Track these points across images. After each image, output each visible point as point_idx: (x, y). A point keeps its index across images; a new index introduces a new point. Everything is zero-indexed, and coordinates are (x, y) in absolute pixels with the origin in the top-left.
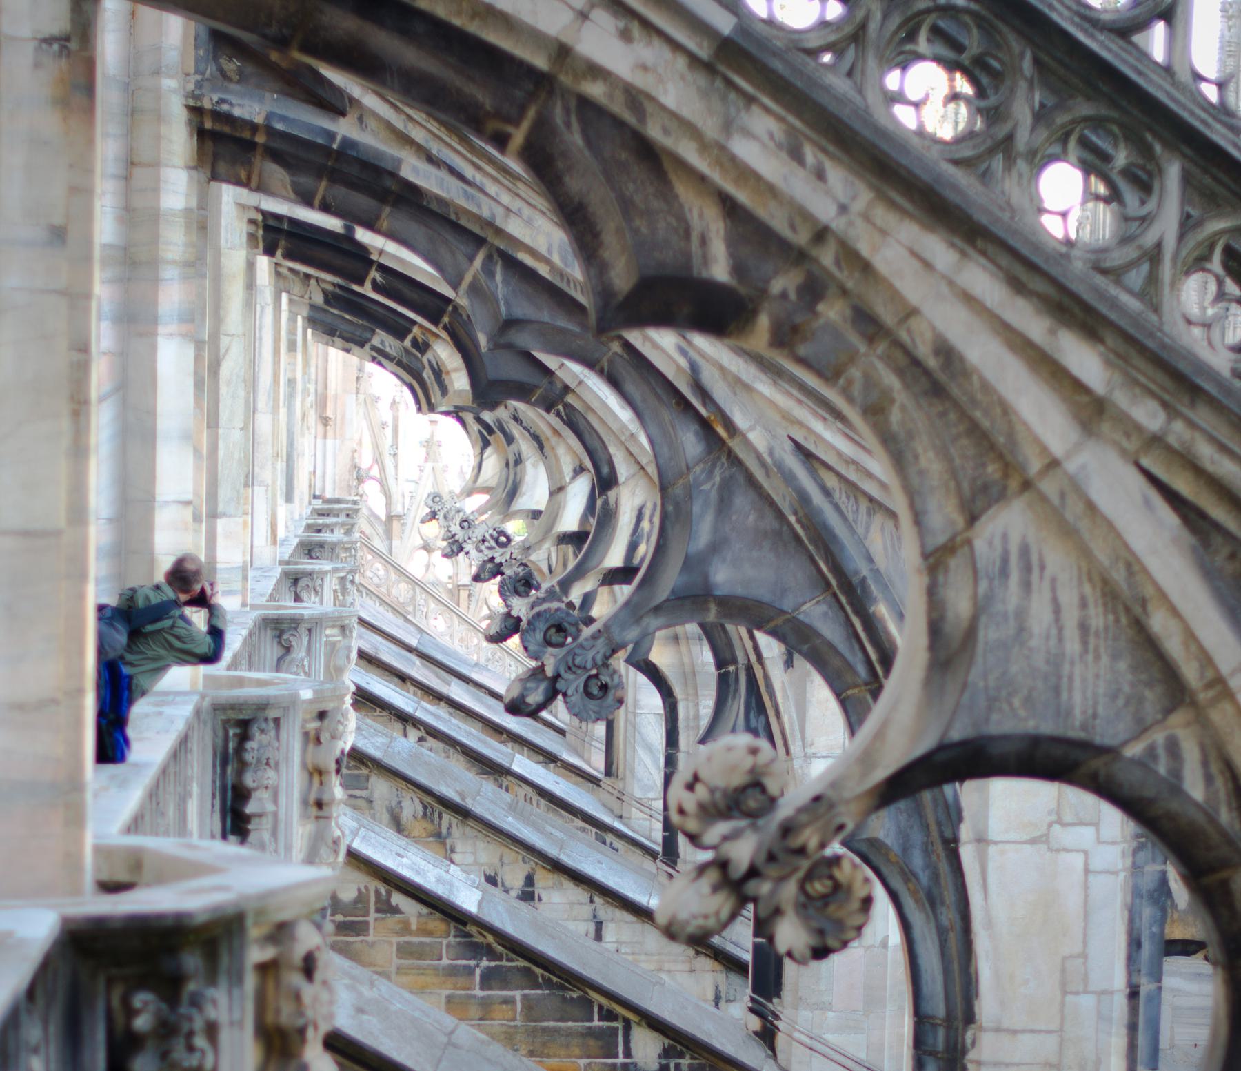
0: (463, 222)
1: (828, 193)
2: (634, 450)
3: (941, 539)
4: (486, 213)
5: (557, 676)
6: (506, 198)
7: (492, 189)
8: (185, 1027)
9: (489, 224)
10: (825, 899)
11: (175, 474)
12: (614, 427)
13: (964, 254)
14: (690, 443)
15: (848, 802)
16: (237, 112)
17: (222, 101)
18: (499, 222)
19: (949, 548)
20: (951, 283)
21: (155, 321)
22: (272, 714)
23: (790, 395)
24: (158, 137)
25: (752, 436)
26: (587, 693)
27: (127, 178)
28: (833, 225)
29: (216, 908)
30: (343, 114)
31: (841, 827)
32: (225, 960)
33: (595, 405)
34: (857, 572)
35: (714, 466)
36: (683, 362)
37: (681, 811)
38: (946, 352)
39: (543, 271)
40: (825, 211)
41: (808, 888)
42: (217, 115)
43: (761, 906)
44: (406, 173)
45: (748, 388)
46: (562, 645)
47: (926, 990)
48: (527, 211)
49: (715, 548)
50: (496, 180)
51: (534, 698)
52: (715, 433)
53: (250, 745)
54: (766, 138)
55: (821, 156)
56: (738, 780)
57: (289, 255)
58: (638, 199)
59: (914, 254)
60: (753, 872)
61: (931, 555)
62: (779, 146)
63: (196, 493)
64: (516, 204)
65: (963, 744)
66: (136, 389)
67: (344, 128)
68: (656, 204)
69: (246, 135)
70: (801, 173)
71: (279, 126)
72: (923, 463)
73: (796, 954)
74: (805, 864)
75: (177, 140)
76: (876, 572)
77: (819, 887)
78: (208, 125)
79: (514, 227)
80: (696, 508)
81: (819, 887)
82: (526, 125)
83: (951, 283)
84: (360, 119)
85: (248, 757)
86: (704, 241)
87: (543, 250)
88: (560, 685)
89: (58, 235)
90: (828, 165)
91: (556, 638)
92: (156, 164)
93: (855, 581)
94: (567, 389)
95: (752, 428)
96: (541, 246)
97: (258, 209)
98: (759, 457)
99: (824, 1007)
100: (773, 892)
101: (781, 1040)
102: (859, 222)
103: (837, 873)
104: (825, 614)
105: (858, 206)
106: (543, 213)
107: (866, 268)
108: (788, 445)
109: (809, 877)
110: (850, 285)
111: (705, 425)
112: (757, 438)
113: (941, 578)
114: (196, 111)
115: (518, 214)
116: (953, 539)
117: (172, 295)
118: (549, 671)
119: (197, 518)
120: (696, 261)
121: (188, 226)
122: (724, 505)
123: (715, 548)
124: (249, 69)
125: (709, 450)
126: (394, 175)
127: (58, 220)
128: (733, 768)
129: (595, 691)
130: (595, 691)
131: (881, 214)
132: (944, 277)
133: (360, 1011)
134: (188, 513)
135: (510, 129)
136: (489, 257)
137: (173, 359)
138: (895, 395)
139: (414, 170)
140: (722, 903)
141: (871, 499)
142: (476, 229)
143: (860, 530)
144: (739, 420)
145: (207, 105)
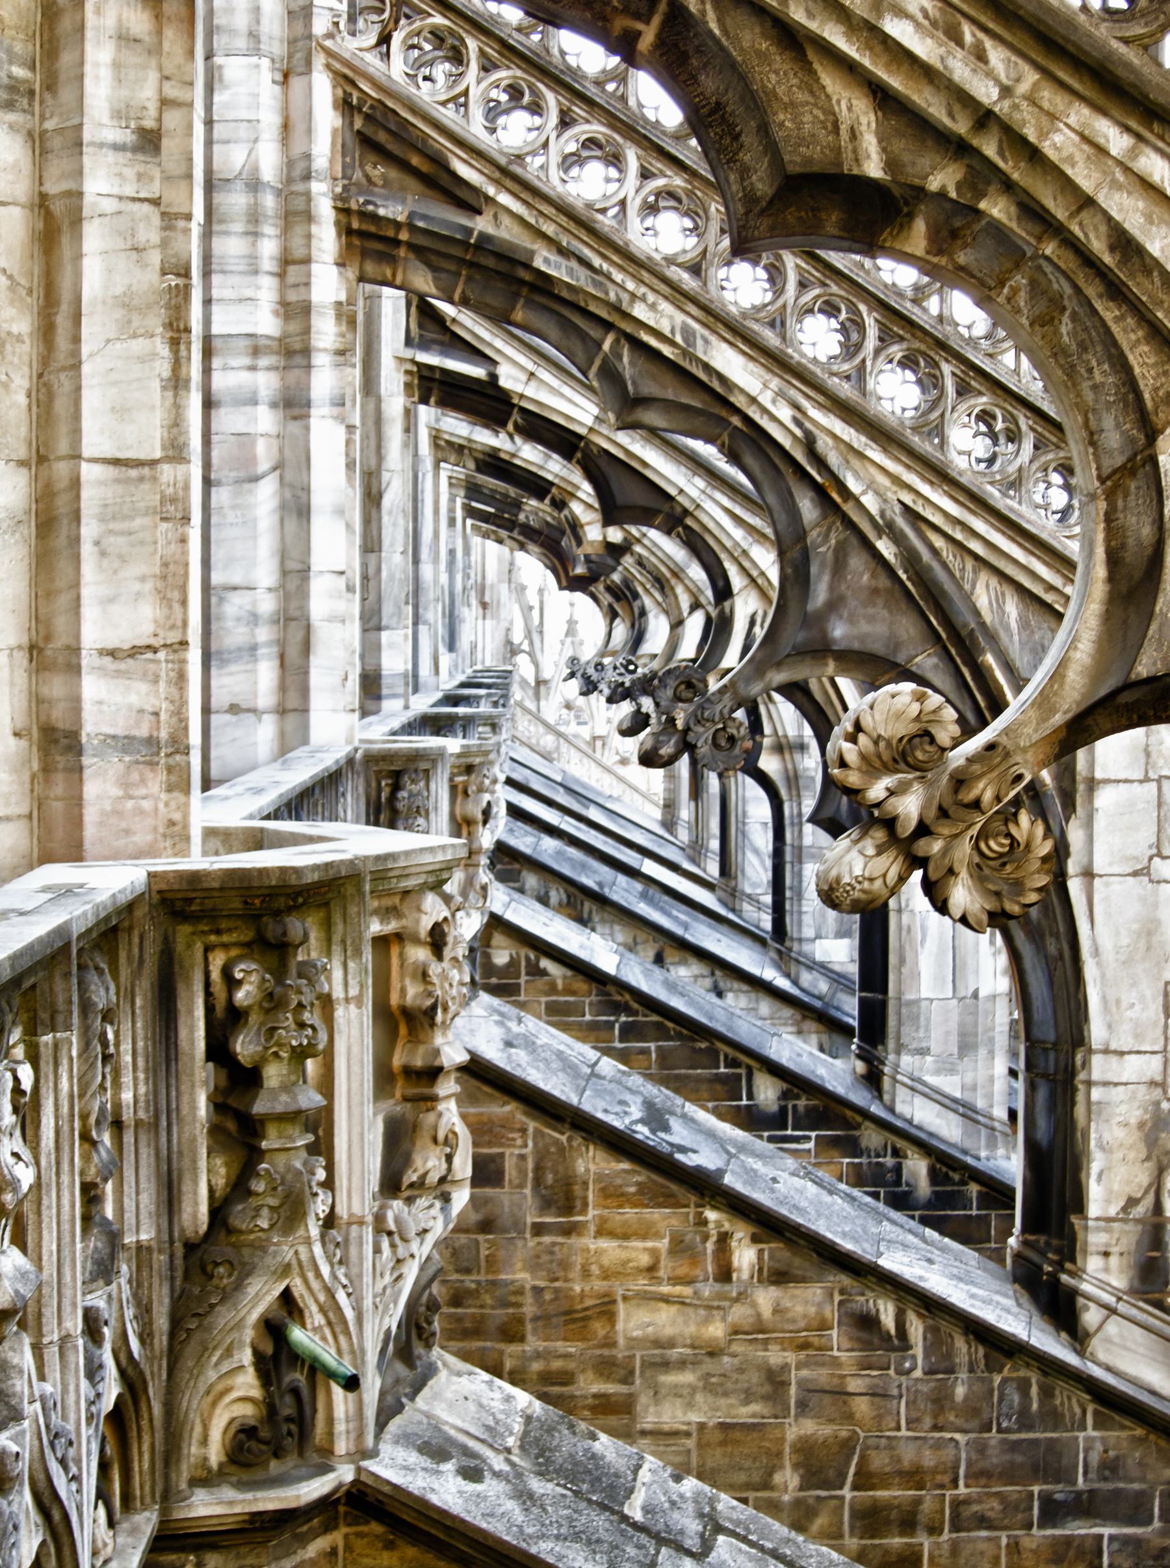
0: (593, 308)
1: (990, 74)
2: (746, 564)
3: (1119, 461)
4: (612, 296)
5: (687, 730)
6: (630, 285)
7: (618, 277)
8: (294, 1000)
9: (617, 308)
10: (1003, 859)
11: (333, 545)
12: (728, 544)
13: (1139, 137)
14: (808, 508)
15: (1024, 750)
16: (381, 212)
17: (367, 202)
18: (625, 306)
19: (1128, 469)
20: (1127, 170)
21: (308, 404)
22: (423, 765)
23: (899, 461)
24: (309, 236)
25: (863, 499)
26: (715, 744)
27: (281, 275)
28: (996, 109)
29: (328, 865)
30: (479, 212)
31: (1019, 777)
32: (339, 929)
33: (711, 525)
34: (965, 625)
35: (829, 530)
36: (798, 432)
37: (843, 764)
38: (1125, 243)
39: (667, 351)
40: (986, 93)
41: (983, 846)
42: (363, 215)
43: (931, 867)
44: (538, 263)
45: (861, 456)
46: (690, 701)
47: (1037, 1017)
48: (651, 298)
49: (834, 605)
50: (621, 268)
51: (666, 751)
52: (832, 497)
53: (403, 794)
54: (920, 17)
55: (981, 35)
56: (902, 729)
57: (443, 403)
58: (781, 90)
59: (1085, 138)
60: (923, 830)
61: (1109, 477)
62: (934, 24)
63: (349, 566)
64: (643, 290)
65: (1151, 680)
66: (294, 471)
67: (482, 224)
68: (801, 96)
69: (390, 233)
70: (959, 53)
71: (421, 224)
72: (1098, 377)
73: (971, 920)
74: (980, 820)
75: (326, 238)
76: (983, 624)
77: (996, 846)
78: (355, 225)
79: (640, 311)
80: (814, 570)
81: (996, 846)
82: (656, 20)
83: (1127, 170)
84: (495, 216)
85: (400, 806)
86: (854, 135)
87: (667, 332)
88: (691, 737)
89: (149, 141)
90: (988, 44)
91: (686, 694)
92: (307, 261)
93: (964, 633)
94: (686, 512)
95: (864, 493)
96: (665, 327)
97: (413, 361)
98: (871, 518)
99: (923, 1052)
100: (945, 851)
101: (886, 1082)
102: (1024, 104)
103: (1013, 830)
104: (936, 666)
105: (1023, 88)
106: (666, 298)
107: (1033, 155)
108: (898, 508)
109: (983, 835)
110: (1015, 176)
111: (820, 492)
112: (870, 502)
113: (1120, 503)
114: (343, 211)
115: (643, 299)
116: (1131, 459)
117: (324, 379)
118: (680, 724)
119: (350, 589)
120: (847, 156)
121: (339, 317)
122: (839, 567)
123: (834, 605)
124: (394, 174)
125: (824, 516)
126: (528, 267)
127: (149, 124)
128: (899, 715)
129: (723, 743)
130: (723, 743)
131: (1049, 96)
132: (1120, 163)
133: (509, 1044)
134: (341, 582)
135: (640, 26)
136: (617, 341)
137: (328, 443)
138: (1066, 302)
139: (545, 261)
140: (889, 865)
141: (976, 557)
142: (603, 313)
143: (967, 587)
144: (853, 485)
145: (354, 206)
